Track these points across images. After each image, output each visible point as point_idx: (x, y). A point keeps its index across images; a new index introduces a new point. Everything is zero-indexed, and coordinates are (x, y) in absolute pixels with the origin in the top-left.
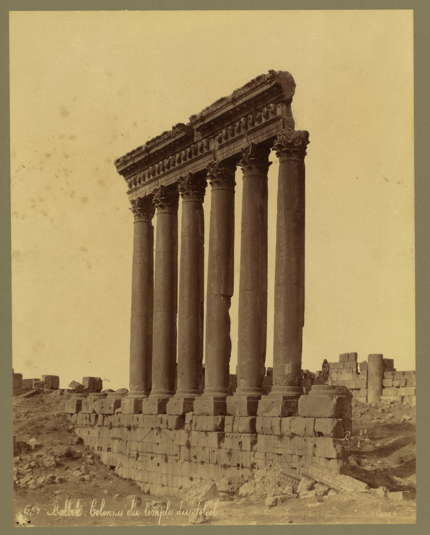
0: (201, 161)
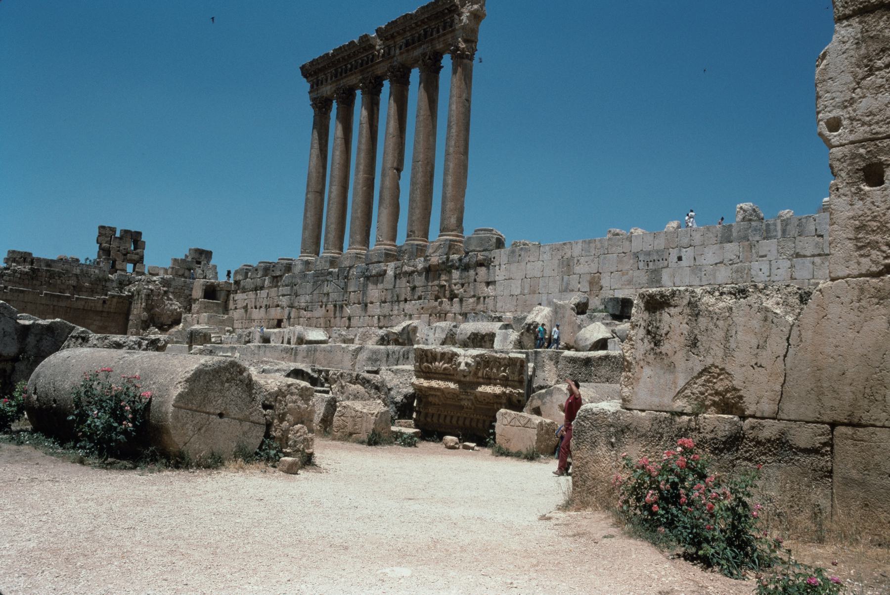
0: (381, 64)
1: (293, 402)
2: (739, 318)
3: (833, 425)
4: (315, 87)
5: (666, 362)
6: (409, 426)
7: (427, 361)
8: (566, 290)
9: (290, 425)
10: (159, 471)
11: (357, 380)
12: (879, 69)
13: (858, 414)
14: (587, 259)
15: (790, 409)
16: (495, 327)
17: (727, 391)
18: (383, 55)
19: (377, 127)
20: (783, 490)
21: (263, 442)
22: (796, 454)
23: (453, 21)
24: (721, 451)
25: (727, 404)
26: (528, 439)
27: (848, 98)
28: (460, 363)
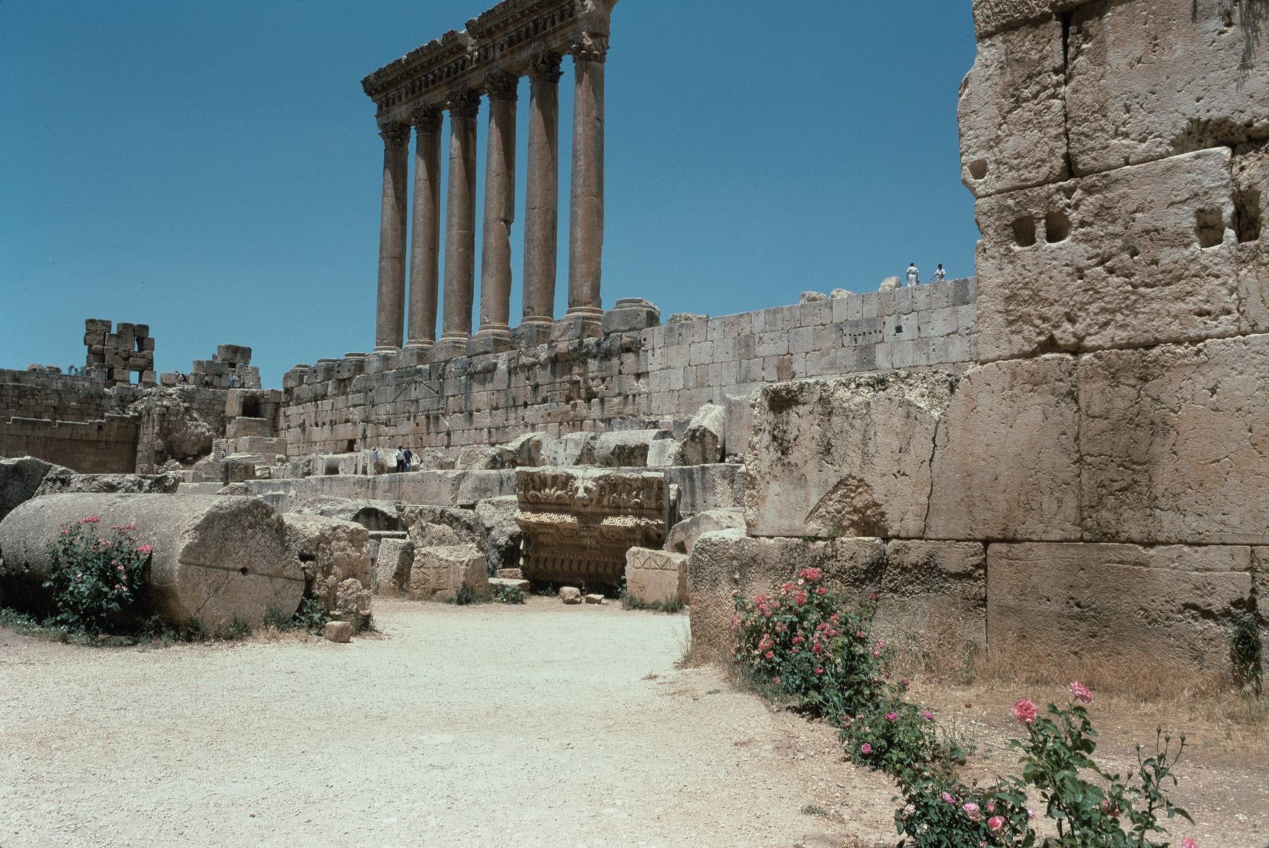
0: (477, 73)
1: (340, 550)
2: (878, 416)
3: (987, 542)
4: (384, 107)
5: (795, 474)
6: (515, 577)
7: (534, 488)
8: (745, 380)
9: (339, 580)
10: (166, 646)
11: (442, 518)
12: (1026, 100)
13: (1012, 528)
14: (772, 335)
15: (939, 526)
16: (648, 436)
17: (867, 507)
18: (478, 60)
19: (474, 161)
20: (931, 627)
21: (302, 604)
22: (946, 580)
23: (573, 8)
24: (863, 582)
25: (867, 523)
26: (668, 586)
27: (993, 136)
28: (577, 489)
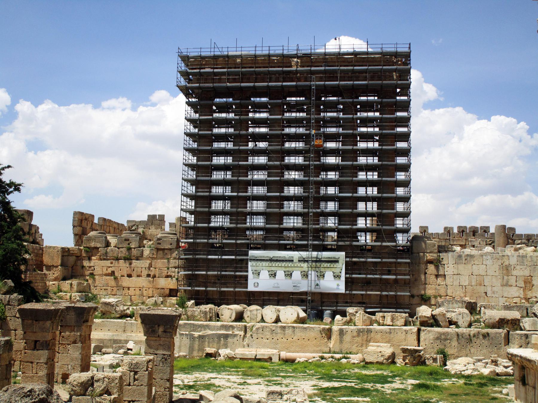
14: (522, 267)
